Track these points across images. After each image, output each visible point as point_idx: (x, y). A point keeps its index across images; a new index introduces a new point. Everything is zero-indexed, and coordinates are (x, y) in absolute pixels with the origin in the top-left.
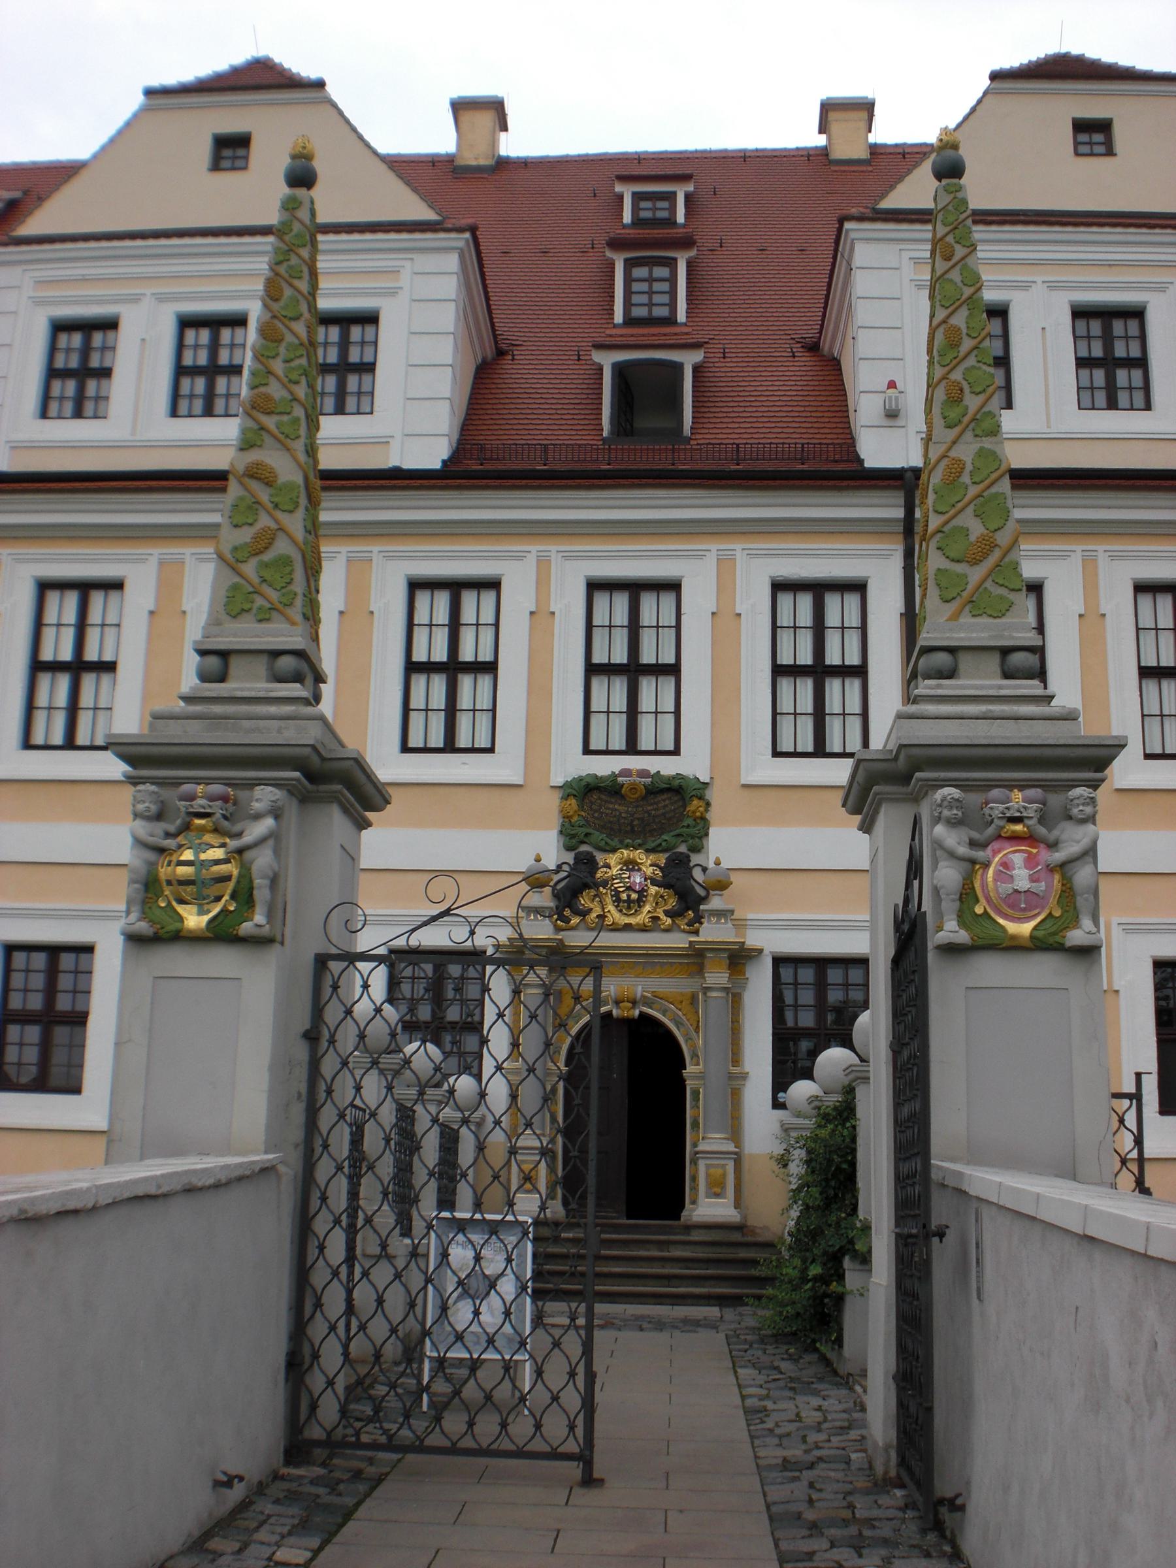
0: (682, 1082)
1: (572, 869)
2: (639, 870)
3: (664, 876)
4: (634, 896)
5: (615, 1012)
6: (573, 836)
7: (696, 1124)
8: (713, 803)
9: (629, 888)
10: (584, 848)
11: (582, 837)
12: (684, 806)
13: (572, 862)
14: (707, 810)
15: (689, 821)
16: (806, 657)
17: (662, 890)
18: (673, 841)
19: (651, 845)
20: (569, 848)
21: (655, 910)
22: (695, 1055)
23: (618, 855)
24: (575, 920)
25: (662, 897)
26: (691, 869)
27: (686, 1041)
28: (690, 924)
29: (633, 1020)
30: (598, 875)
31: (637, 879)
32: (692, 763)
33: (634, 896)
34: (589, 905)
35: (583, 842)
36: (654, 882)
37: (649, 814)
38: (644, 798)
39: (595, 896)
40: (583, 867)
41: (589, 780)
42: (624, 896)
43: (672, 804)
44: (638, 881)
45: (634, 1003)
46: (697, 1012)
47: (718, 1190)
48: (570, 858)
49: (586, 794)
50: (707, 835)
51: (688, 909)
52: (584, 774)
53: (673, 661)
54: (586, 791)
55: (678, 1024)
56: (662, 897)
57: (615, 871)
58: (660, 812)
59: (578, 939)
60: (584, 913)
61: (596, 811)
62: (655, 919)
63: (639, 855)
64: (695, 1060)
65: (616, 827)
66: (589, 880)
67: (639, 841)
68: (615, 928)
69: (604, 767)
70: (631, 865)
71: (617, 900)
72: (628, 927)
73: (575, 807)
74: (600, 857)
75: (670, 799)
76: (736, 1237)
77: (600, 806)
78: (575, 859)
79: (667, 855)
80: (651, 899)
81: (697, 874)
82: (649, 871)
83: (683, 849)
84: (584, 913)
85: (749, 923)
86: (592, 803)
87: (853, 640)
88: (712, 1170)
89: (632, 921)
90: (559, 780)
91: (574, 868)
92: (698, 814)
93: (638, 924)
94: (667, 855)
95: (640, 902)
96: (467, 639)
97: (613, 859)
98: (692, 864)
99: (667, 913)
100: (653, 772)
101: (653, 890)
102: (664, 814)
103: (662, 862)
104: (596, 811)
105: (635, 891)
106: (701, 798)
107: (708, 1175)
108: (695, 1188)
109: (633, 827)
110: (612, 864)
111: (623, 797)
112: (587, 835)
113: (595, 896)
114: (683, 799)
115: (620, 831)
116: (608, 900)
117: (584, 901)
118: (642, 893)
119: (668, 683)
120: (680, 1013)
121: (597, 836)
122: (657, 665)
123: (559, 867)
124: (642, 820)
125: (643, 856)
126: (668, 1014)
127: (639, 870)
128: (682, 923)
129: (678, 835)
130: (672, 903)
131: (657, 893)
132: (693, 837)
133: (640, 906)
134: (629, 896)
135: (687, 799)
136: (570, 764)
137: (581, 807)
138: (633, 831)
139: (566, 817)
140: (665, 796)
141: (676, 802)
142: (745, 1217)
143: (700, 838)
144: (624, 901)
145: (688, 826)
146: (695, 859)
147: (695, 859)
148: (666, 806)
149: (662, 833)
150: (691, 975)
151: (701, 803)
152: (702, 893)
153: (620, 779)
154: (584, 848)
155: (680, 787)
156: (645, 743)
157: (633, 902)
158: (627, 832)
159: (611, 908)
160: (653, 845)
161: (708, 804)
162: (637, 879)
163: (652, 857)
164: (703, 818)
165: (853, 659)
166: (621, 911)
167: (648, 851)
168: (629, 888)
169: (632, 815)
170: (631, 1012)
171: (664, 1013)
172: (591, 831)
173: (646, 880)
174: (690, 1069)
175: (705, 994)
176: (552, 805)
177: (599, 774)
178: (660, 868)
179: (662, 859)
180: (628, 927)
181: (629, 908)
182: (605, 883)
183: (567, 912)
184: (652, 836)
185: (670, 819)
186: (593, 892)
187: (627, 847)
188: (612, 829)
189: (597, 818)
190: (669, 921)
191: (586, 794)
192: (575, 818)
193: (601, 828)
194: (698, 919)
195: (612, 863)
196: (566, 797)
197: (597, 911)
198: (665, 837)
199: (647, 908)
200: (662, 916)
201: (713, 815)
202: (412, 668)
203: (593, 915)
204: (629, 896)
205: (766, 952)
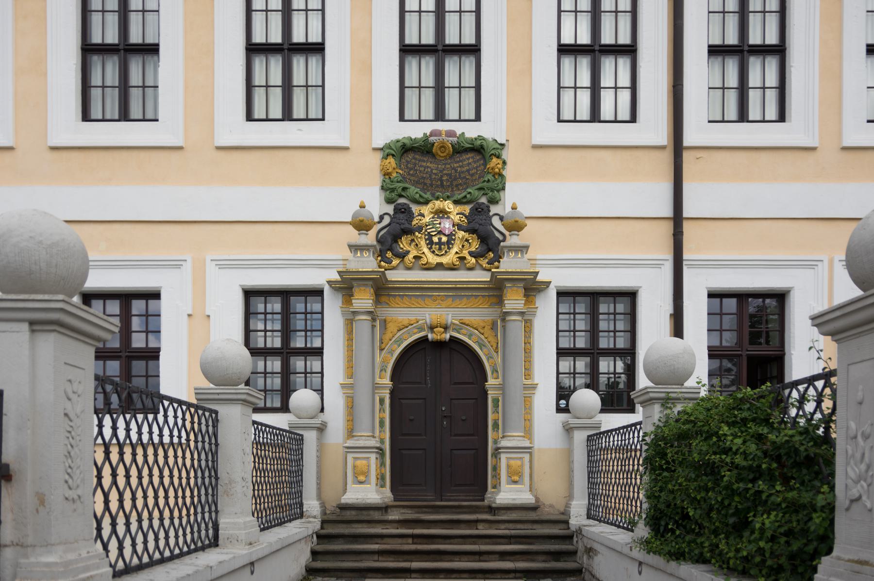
0: (485, 393)
1: (392, 218)
2: (448, 218)
3: (469, 223)
4: (444, 239)
5: (430, 336)
6: (392, 190)
7: (496, 425)
8: (508, 162)
9: (440, 232)
10: (402, 201)
11: (400, 190)
12: (485, 164)
13: (392, 213)
14: (503, 168)
15: (490, 177)
16: (584, 38)
17: (466, 235)
18: (477, 193)
19: (458, 196)
20: (389, 201)
21: (461, 251)
22: (495, 371)
23: (430, 205)
24: (396, 262)
25: (467, 240)
26: (491, 218)
27: (488, 360)
28: (491, 262)
29: (445, 342)
30: (414, 223)
31: (447, 225)
32: (488, 129)
33: (444, 239)
34: (407, 248)
35: (401, 196)
36: (460, 227)
37: (456, 171)
38: (451, 157)
39: (413, 240)
40: (402, 216)
41: (407, 142)
42: (435, 239)
43: (475, 162)
44: (447, 226)
45: (446, 328)
46: (496, 336)
47: (516, 478)
48: (390, 209)
49: (402, 155)
50: (503, 189)
51: (489, 250)
52: (400, 138)
53: (473, 42)
54: (405, 151)
55: (481, 346)
56: (467, 240)
57: (427, 219)
58: (465, 169)
59: (397, 276)
60: (402, 256)
61: (411, 169)
62: (462, 259)
63: (448, 205)
64: (495, 374)
65: (428, 182)
66: (407, 225)
67: (448, 194)
68: (428, 268)
69: (416, 131)
70: (441, 213)
71: (430, 243)
72: (439, 266)
73: (394, 165)
74: (415, 209)
75: (472, 157)
76: (532, 516)
77: (415, 164)
78: (394, 210)
79: (471, 206)
80: (457, 242)
81: (496, 221)
82: (457, 219)
83: (483, 200)
84: (402, 256)
85: (538, 262)
86: (407, 162)
87: (625, 22)
88: (512, 462)
89: (445, 260)
90: (380, 144)
91: (393, 218)
92: (497, 170)
93: (447, 264)
94: (471, 206)
95: (449, 244)
96: (298, 21)
97: (426, 210)
98: (491, 214)
99: (471, 254)
100: (458, 133)
101: (461, 234)
102: (468, 171)
103: (467, 212)
104: (411, 169)
105: (445, 235)
106: (498, 157)
107: (508, 466)
108: (497, 476)
109: (442, 181)
110: (424, 214)
111: (434, 156)
112: (404, 189)
113: (413, 240)
114: (484, 158)
115: (431, 185)
116: (423, 243)
117: (404, 244)
118: (451, 236)
119: (468, 63)
120: (482, 337)
121: (413, 190)
122: (460, 45)
123: (381, 218)
124: (449, 175)
125: (451, 206)
126: (474, 337)
127: (448, 218)
128: (484, 262)
129: (480, 189)
130: (475, 245)
131: (463, 237)
132: (492, 190)
133: (449, 248)
134: (440, 239)
135: (487, 156)
136: (390, 130)
137: (399, 166)
138: (442, 185)
139: (386, 174)
140: (470, 155)
141: (478, 161)
142: (537, 499)
143: (498, 191)
144: (436, 244)
145: (489, 181)
146: (494, 209)
147: (494, 209)
148: (469, 164)
149: (467, 188)
150: (492, 305)
151: (499, 161)
152: (501, 238)
153: (432, 139)
154: (402, 201)
155: (482, 147)
156: (452, 111)
157: (443, 244)
158: (437, 186)
159: (426, 250)
160: (460, 197)
161: (504, 163)
162: (447, 225)
163: (459, 208)
164: (501, 175)
165: (624, 39)
166: (433, 252)
167: (456, 202)
168: (440, 232)
169: (441, 171)
170: (443, 336)
171: (470, 337)
172: (407, 185)
173: (454, 226)
174: (491, 381)
175: (503, 320)
176: (375, 162)
177: (413, 137)
178: (466, 217)
179: (467, 209)
180: (439, 266)
181: (440, 249)
182: (420, 229)
183: (389, 254)
184: (459, 190)
185: (472, 175)
186: (410, 237)
187: (437, 199)
188: (425, 184)
189: (412, 175)
190: (474, 260)
191: (402, 155)
192: (394, 175)
193: (416, 184)
194: (498, 258)
195: (426, 213)
196: (385, 157)
197: (413, 253)
198: (469, 190)
199: (455, 249)
200: (468, 257)
201: (508, 173)
202: (253, 49)
203: (411, 256)
204: (440, 239)
205: (552, 286)
